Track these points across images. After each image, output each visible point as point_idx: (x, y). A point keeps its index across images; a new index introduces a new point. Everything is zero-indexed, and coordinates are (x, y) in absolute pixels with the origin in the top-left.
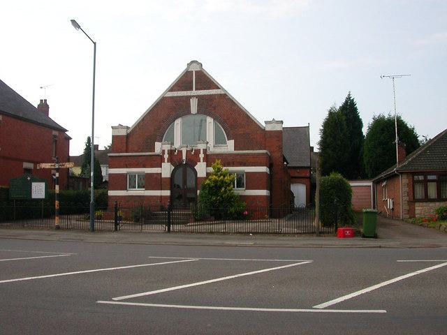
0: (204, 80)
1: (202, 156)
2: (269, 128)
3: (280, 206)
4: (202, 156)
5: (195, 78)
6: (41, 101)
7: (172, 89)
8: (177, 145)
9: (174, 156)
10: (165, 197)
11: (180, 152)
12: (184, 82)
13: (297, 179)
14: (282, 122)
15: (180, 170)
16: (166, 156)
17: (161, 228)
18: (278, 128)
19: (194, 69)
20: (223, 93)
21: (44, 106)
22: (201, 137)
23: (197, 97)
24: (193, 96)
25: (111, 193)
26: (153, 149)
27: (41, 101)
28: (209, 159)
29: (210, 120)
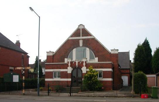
0: (85, 33)
1: (84, 64)
2: (112, 52)
3: (117, 85)
4: (84, 64)
5: (82, 32)
6: (17, 41)
7: (72, 36)
8: (74, 59)
9: (73, 64)
10: (69, 81)
11: (75, 63)
12: (77, 33)
13: (124, 74)
14: (118, 50)
15: (75, 70)
16: (69, 64)
17: (68, 94)
18: (116, 52)
19: (81, 28)
20: (93, 38)
21: (18, 43)
22: (84, 56)
23: (82, 39)
24: (81, 39)
25: (46, 80)
26: (64, 61)
27: (17, 41)
28: (87, 66)
29: (88, 49)
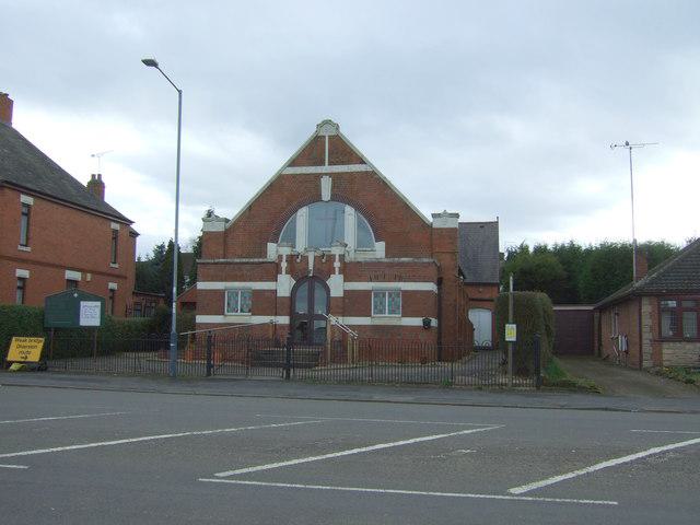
0: (342, 151)
1: (337, 264)
2: (437, 224)
3: (448, 342)
4: (337, 264)
5: (328, 147)
6: (93, 176)
7: (293, 163)
8: (301, 246)
9: (295, 265)
10: (282, 326)
11: (305, 259)
12: (312, 152)
13: (479, 302)
14: (457, 216)
15: (304, 291)
16: (284, 265)
17: (278, 373)
18: (452, 224)
19: (327, 133)
20: (369, 169)
21: (97, 185)
22: (336, 236)
23: (330, 175)
24: (326, 174)
25: (200, 319)
26: (264, 253)
27: (93, 176)
28: (351, 271)
29: (349, 210)
